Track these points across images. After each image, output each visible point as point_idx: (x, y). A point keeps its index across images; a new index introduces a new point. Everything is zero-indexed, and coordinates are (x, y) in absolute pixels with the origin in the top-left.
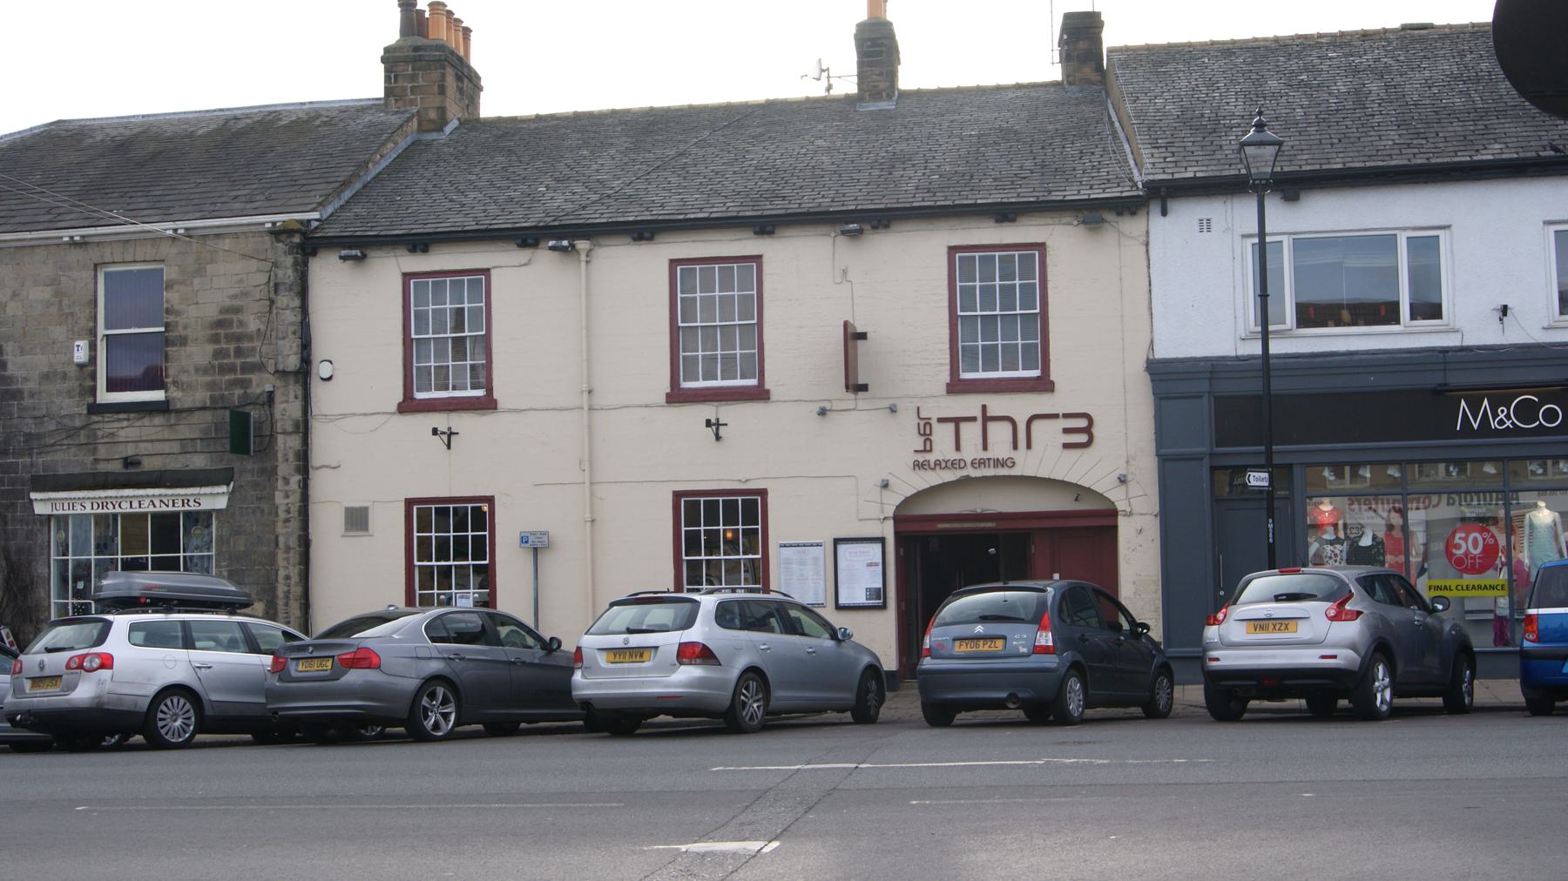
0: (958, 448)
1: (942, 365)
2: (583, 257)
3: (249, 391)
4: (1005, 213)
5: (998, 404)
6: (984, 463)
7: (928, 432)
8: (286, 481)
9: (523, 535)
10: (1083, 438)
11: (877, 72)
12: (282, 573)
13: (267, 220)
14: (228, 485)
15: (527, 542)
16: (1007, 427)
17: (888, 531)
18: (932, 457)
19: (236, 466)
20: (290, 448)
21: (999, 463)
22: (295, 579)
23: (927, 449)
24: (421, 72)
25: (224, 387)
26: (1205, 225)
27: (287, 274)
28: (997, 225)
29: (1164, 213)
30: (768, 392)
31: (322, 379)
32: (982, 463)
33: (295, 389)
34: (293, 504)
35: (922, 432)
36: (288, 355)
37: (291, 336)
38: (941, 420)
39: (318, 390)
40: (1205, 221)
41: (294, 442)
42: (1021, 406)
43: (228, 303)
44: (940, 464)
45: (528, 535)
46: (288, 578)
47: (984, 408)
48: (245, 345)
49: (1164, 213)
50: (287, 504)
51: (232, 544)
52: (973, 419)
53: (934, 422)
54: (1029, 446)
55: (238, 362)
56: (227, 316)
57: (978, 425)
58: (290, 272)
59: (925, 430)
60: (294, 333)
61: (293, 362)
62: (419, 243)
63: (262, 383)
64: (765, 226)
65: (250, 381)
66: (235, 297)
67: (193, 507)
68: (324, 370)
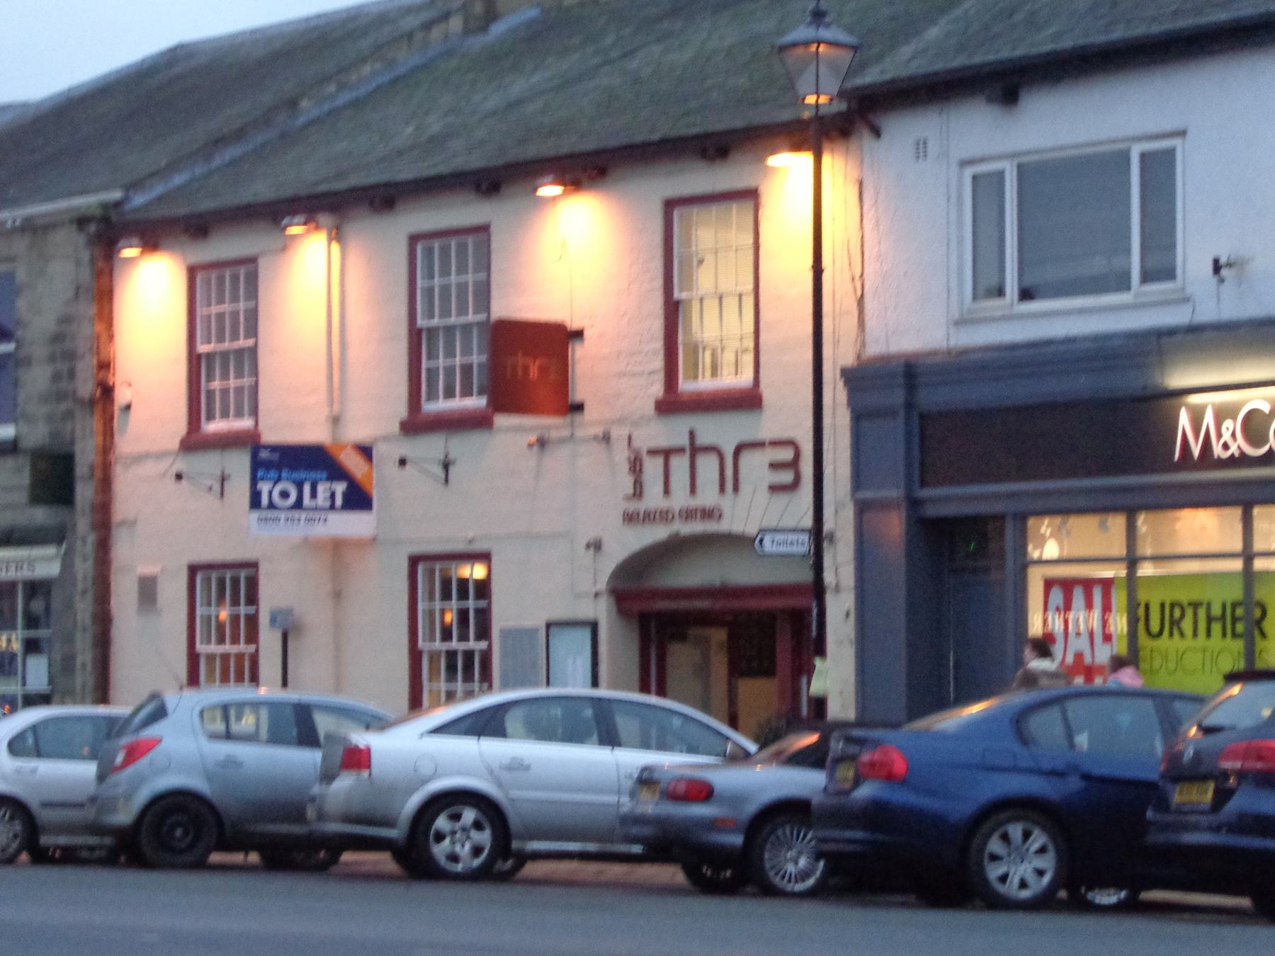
0: (667, 491)
1: (652, 373)
8: (84, 541)
12: (79, 661)
17: (602, 611)
21: (708, 514)
23: (638, 491)
26: (921, 148)
29: (877, 133)
32: (689, 515)
38: (653, 452)
47: (692, 435)
49: (877, 133)
52: (680, 450)
54: (736, 488)
59: (636, 466)
67: (26, 574)
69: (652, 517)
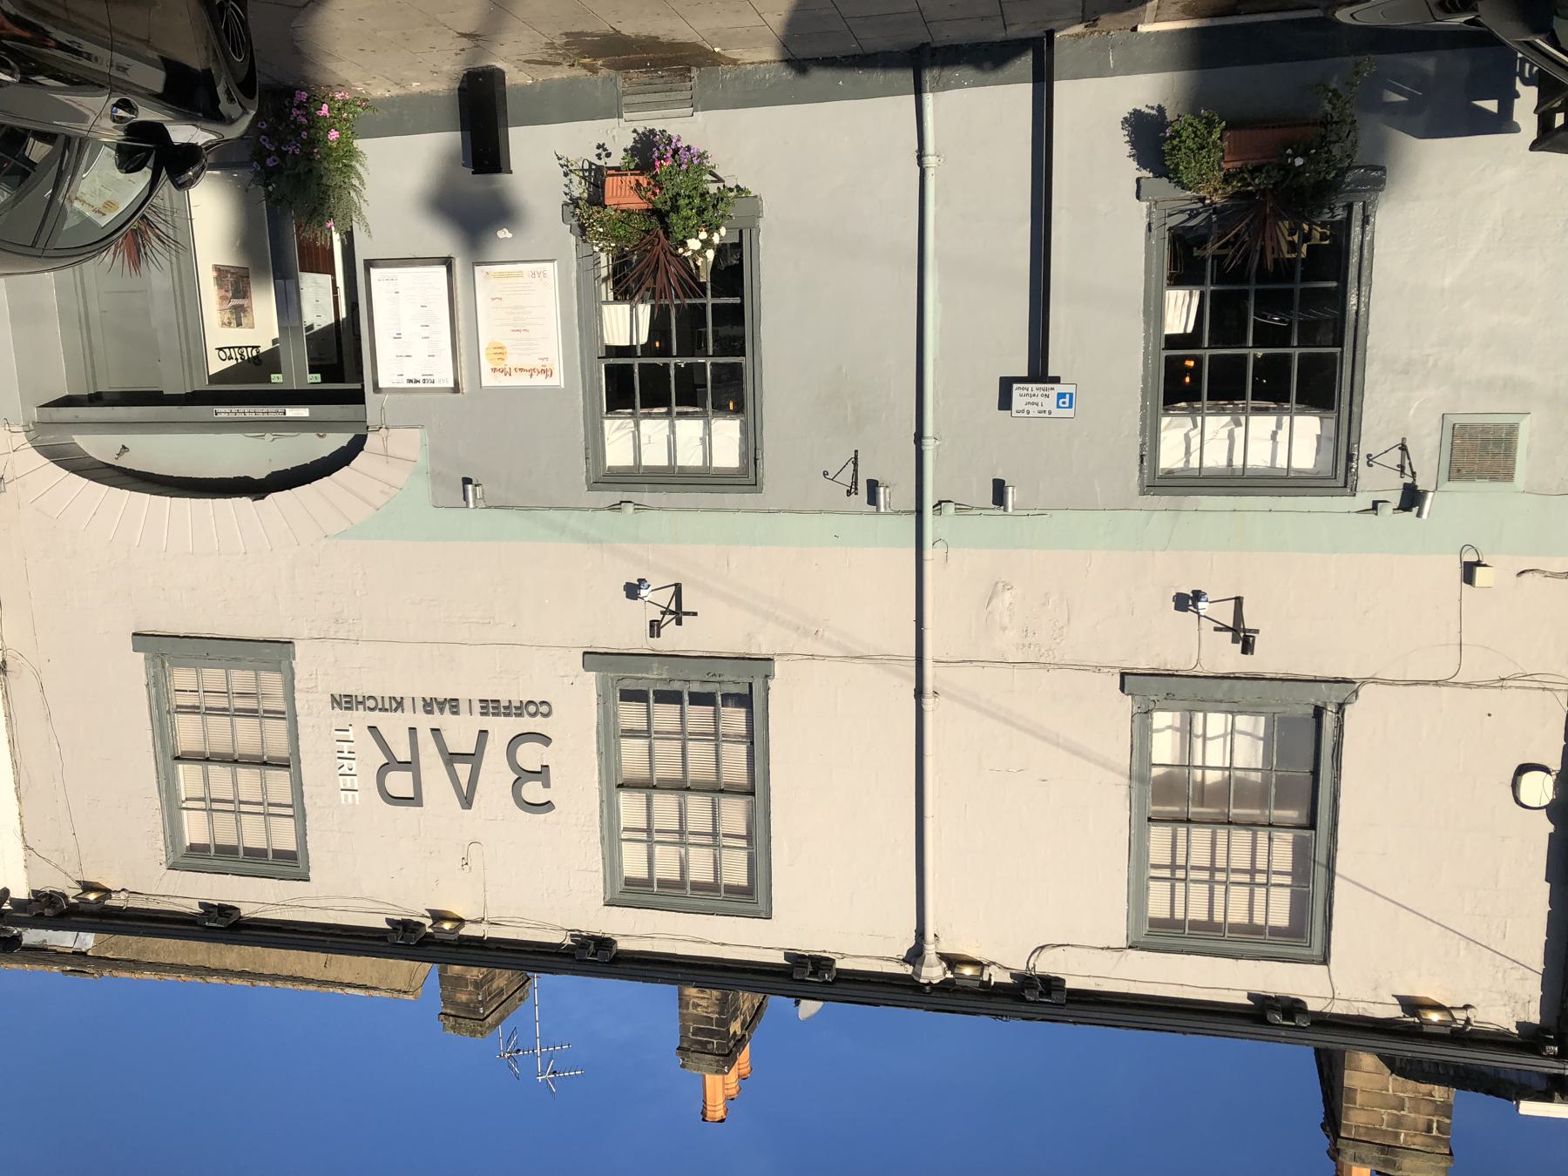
9: (1069, 413)
11: (699, 1009)
24: (1384, 1127)
30: (586, 666)
45: (1057, 413)
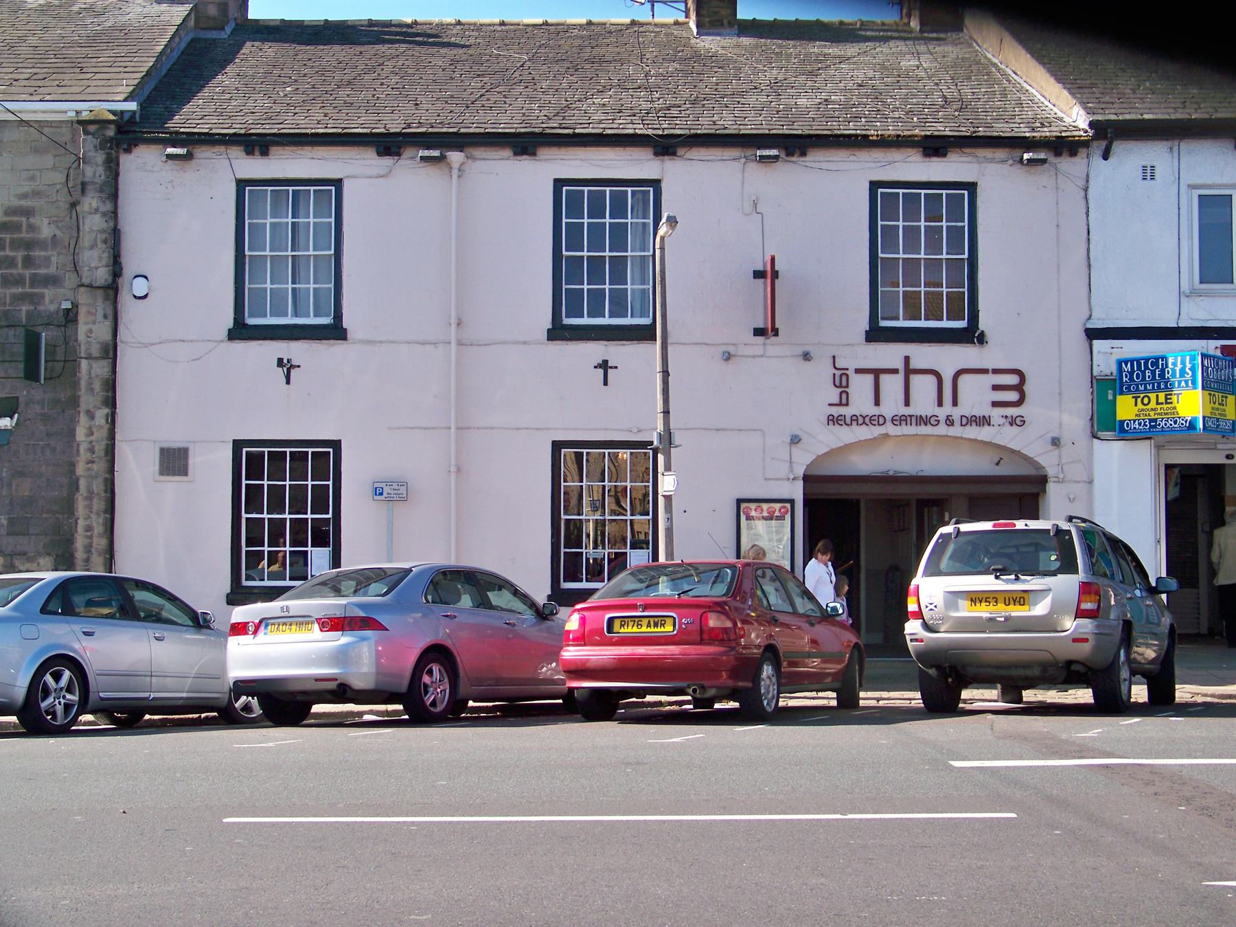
0: (877, 403)
2: (455, 172)
3: (41, 308)
4: (935, 147)
5: (923, 355)
6: (906, 420)
7: (844, 383)
8: (91, 416)
9: (376, 485)
10: (1013, 396)
13: (69, 110)
14: (12, 418)
15: (381, 494)
16: (931, 380)
17: (797, 492)
18: (847, 412)
19: (23, 394)
20: (97, 376)
21: (923, 420)
22: (98, 529)
23: (844, 401)
25: (8, 301)
26: (1148, 173)
27: (95, 171)
28: (927, 159)
29: (1106, 157)
31: (135, 297)
32: (899, 420)
33: (101, 307)
34: (97, 441)
35: (837, 383)
36: (97, 268)
37: (101, 245)
38: (858, 371)
39: (130, 311)
40: (1149, 168)
41: (101, 369)
42: (948, 358)
43: (16, 202)
44: (857, 420)
45: (383, 485)
46: (89, 528)
47: (907, 359)
48: (37, 253)
50: (91, 442)
51: (14, 487)
52: (895, 371)
53: (851, 373)
55: (27, 273)
56: (15, 219)
57: (898, 379)
58: (101, 170)
59: (841, 381)
60: (105, 241)
61: (102, 275)
62: (257, 144)
63: (54, 300)
64: (666, 146)
65: (42, 296)
66: (24, 196)
68: (140, 287)
69: (914, 419)
